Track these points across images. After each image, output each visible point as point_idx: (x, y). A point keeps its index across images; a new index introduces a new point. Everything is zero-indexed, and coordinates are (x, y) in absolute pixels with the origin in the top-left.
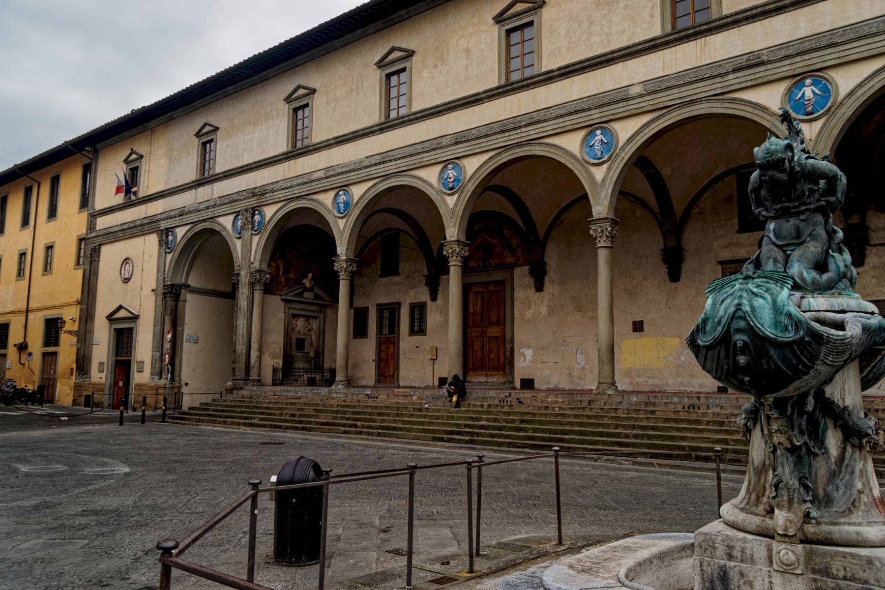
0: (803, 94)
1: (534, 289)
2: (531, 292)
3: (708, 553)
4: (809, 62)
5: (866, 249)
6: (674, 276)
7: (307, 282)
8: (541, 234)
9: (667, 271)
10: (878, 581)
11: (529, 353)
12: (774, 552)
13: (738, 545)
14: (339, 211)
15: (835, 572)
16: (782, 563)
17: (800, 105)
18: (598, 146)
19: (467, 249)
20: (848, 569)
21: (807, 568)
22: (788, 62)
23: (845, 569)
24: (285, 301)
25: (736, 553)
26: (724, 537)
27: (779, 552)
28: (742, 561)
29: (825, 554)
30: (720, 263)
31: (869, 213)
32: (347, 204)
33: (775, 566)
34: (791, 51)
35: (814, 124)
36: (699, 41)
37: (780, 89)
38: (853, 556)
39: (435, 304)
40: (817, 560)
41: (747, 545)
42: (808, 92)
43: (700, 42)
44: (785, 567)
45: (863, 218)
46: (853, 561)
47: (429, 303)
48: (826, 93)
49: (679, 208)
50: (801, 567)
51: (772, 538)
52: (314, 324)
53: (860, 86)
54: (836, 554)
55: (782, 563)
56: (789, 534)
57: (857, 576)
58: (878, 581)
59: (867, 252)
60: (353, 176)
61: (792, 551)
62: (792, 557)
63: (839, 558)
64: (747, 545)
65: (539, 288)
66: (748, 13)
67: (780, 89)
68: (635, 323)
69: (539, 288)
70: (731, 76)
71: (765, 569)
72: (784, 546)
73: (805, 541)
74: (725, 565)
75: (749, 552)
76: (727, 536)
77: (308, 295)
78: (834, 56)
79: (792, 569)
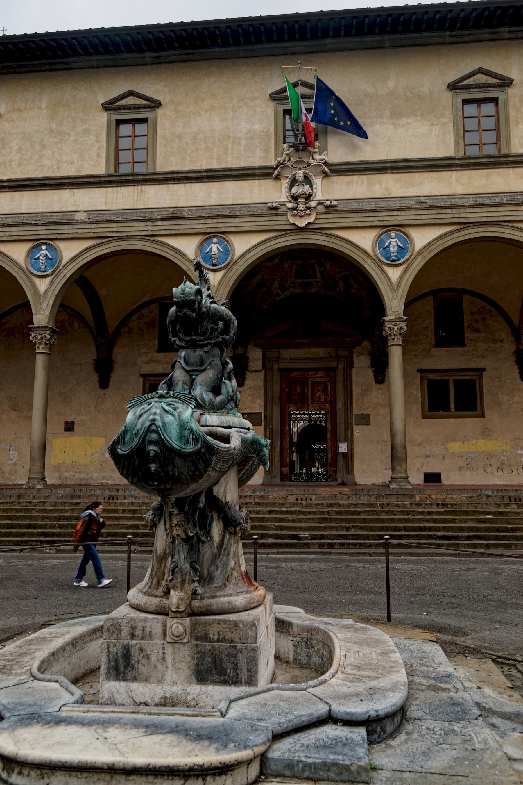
0: (211, 248)
3: (115, 635)
4: (216, 225)
5: (245, 374)
6: (104, 384)
9: (98, 379)
10: (240, 639)
12: (168, 627)
13: (140, 625)
15: (211, 637)
16: (174, 635)
17: (208, 256)
18: (42, 260)
20: (221, 633)
21: (192, 636)
22: (202, 221)
23: (219, 633)
25: (138, 632)
26: (129, 620)
27: (171, 627)
28: (142, 638)
29: (205, 623)
30: (142, 375)
31: (250, 347)
33: (168, 639)
34: (203, 214)
35: (217, 273)
36: (136, 187)
37: (196, 241)
38: (224, 621)
40: (200, 628)
41: (147, 624)
42: (215, 248)
43: (137, 189)
44: (175, 638)
45: (246, 350)
46: (225, 626)
48: (227, 251)
49: (112, 326)
50: (188, 636)
51: (167, 615)
53: (249, 251)
54: (213, 621)
55: (174, 635)
56: (181, 610)
57: (226, 638)
58: (240, 639)
59: (247, 376)
61: (182, 624)
62: (181, 629)
63: (215, 625)
64: (147, 624)
66: (176, 176)
67: (196, 241)
68: (67, 423)
70: (159, 223)
71: (160, 642)
72: (176, 620)
73: (192, 614)
74: (128, 644)
75: (148, 629)
76: (131, 618)
78: (233, 225)
79: (180, 640)
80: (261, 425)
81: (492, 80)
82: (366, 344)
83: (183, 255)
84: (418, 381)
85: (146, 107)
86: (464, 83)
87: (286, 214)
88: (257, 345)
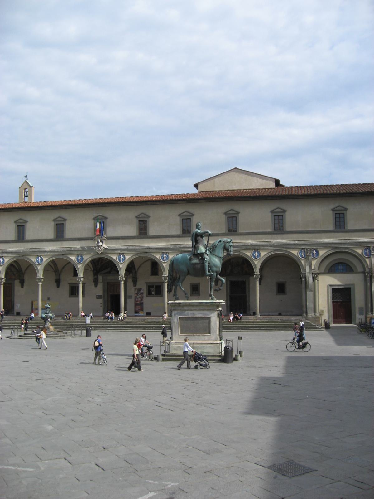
2: (20, 288)
6: (58, 286)
8: (23, 271)
11: (19, 305)
19: (5, 280)
31: (99, 275)
45: (97, 276)
49: (60, 269)
65: (22, 286)
69: (22, 286)
70: (66, 252)
80: (101, 298)
81: (145, 216)
82: (131, 275)
83: (72, 260)
84: (145, 286)
85: (63, 221)
86: (138, 216)
87: (96, 250)
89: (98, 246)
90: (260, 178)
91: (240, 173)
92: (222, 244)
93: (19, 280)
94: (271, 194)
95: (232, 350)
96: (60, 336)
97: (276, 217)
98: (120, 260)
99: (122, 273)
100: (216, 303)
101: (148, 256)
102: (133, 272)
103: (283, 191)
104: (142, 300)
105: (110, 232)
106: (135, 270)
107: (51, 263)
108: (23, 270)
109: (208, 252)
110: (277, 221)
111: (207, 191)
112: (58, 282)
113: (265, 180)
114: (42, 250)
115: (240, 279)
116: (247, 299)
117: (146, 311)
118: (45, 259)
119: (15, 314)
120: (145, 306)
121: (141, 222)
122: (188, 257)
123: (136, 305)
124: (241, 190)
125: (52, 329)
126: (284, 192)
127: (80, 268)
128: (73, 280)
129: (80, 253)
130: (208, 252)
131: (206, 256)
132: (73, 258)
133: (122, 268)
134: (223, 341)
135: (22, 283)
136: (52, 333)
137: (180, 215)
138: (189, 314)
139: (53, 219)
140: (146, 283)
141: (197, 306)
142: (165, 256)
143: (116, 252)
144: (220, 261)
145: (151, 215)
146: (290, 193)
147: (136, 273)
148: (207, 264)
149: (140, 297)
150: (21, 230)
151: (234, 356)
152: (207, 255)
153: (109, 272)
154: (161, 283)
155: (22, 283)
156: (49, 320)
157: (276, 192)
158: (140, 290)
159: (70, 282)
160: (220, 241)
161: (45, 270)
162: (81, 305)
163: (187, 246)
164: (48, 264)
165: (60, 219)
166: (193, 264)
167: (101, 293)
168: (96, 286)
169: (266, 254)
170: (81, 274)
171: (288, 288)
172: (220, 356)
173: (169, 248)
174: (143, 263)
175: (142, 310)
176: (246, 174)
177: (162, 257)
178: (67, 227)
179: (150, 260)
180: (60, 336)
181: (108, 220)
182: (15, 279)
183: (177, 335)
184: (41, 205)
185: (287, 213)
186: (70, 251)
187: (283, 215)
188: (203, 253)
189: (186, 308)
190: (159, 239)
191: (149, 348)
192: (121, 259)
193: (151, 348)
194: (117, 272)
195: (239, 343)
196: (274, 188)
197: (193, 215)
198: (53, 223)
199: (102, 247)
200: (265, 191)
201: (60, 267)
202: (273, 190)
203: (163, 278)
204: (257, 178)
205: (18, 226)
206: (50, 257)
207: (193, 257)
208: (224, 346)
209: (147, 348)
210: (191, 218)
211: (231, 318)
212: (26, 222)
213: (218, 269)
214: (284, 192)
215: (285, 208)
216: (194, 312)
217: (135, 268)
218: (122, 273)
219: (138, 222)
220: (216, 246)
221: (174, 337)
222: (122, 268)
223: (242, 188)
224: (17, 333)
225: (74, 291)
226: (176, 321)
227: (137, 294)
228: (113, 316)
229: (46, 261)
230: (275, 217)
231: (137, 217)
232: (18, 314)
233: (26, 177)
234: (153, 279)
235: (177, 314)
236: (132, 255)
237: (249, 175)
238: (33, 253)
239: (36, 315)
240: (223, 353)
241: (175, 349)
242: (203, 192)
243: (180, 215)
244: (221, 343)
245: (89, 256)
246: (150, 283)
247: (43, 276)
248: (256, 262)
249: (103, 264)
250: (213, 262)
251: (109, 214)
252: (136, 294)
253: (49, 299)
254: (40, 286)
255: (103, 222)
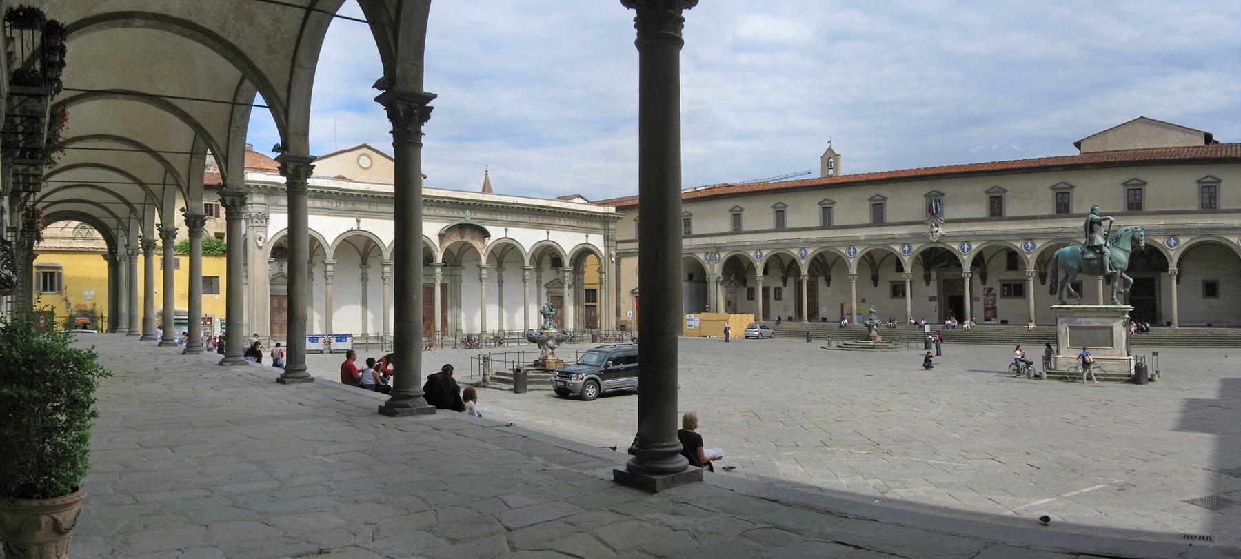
1: (826, 286)
6: (876, 285)
7: (732, 278)
8: (830, 265)
14: (757, 258)
17: (904, 252)
24: (725, 287)
31: (931, 271)
32: (760, 256)
39: (785, 289)
47: (783, 288)
49: (877, 263)
52: (733, 295)
60: (763, 247)
65: (828, 285)
69: (828, 285)
77: (733, 283)
80: (936, 301)
81: (1001, 190)
82: (978, 268)
83: (896, 251)
84: (999, 285)
88: (933, 270)
89: (932, 232)
90: (1182, 131)
91: (1148, 124)
92: (1129, 234)
93: (823, 278)
94: (1198, 156)
95: (1146, 367)
96: (892, 348)
97: (1206, 190)
98: (963, 250)
99: (967, 267)
100: (1121, 308)
101: (1004, 244)
102: (981, 265)
103: (1217, 152)
104: (994, 303)
105: (949, 212)
106: (984, 263)
107: (866, 257)
108: (830, 264)
109: (1108, 244)
110: (1206, 195)
111: (1094, 152)
112: (875, 279)
113: (1188, 135)
114: (856, 238)
115: (1147, 275)
116: (1157, 303)
117: (1000, 317)
118: (859, 250)
119: (820, 320)
120: (998, 311)
121: (993, 199)
122: (1080, 250)
123: (986, 309)
124: (1148, 149)
125: (879, 338)
126: (1219, 153)
127: (907, 261)
128: (897, 277)
129: (905, 241)
130: (1108, 244)
131: (1105, 249)
132: (897, 248)
133: (967, 261)
134: (1132, 357)
135: (828, 281)
136: (880, 344)
137: (1052, 188)
138: (1083, 322)
139: (868, 197)
140: (1000, 280)
141: (1093, 312)
142: (1030, 244)
143: (958, 239)
144: (1126, 255)
145: (1008, 188)
146: (1228, 155)
147: (985, 267)
148: (1107, 259)
149: (991, 300)
150: (827, 212)
151: (1149, 377)
152: (1108, 248)
153: (947, 266)
154: (1022, 280)
155: (828, 281)
156: (875, 327)
157: (1206, 153)
158: (992, 289)
159: (891, 279)
160: (1126, 230)
161: (859, 264)
162: (909, 309)
163: (1064, 231)
164: (863, 257)
165: (878, 198)
166: (1087, 259)
167: (935, 294)
168: (928, 284)
169: (1188, 242)
170: (908, 269)
171: (1222, 289)
172: (1129, 376)
173: (1035, 234)
174: (996, 253)
175: (995, 316)
176: (1158, 126)
177: (1024, 246)
178: (887, 207)
179: (1003, 250)
180: (892, 348)
181: (945, 197)
182: (818, 276)
183: (1066, 348)
184: (851, 180)
185: (1222, 184)
186: (893, 239)
187: (1215, 187)
188: (1102, 245)
189: (1077, 314)
190: (1019, 221)
191: (1029, 364)
192: (966, 249)
193: (1032, 363)
194: (959, 266)
195: (1155, 363)
196: (1203, 147)
197: (1073, 187)
198: (868, 204)
199: (938, 234)
200: (1189, 150)
201: (877, 259)
202: (1201, 149)
203: (1027, 274)
204: (1176, 131)
205: (823, 208)
206: (866, 247)
207: (1086, 250)
208: (1133, 363)
209: (1024, 363)
210: (1070, 191)
211: (1133, 329)
212: (834, 203)
213: (1123, 266)
214: (1219, 153)
215: (1219, 176)
216: (1089, 320)
217: (983, 259)
218: (967, 267)
219: (989, 198)
220: (1121, 236)
221: (1061, 351)
222: (967, 261)
223: (1152, 147)
224: (834, 344)
225: (898, 291)
226: (1064, 330)
227: (987, 295)
228: (956, 324)
229: (861, 252)
230: (1204, 189)
231: (987, 192)
232: (824, 320)
233: (829, 142)
234: (1011, 276)
235: (1065, 322)
236: (981, 243)
237: (1162, 127)
238: (844, 242)
239: (850, 321)
240: (1133, 371)
241: (1064, 366)
242: (1088, 153)
243: (1052, 188)
244: (1130, 359)
245: (919, 245)
246: (1004, 280)
247: (857, 271)
248: (1172, 253)
249: (936, 255)
250: (1116, 256)
251: (947, 188)
252: (985, 295)
253: (863, 301)
254: (854, 285)
255: (939, 200)
